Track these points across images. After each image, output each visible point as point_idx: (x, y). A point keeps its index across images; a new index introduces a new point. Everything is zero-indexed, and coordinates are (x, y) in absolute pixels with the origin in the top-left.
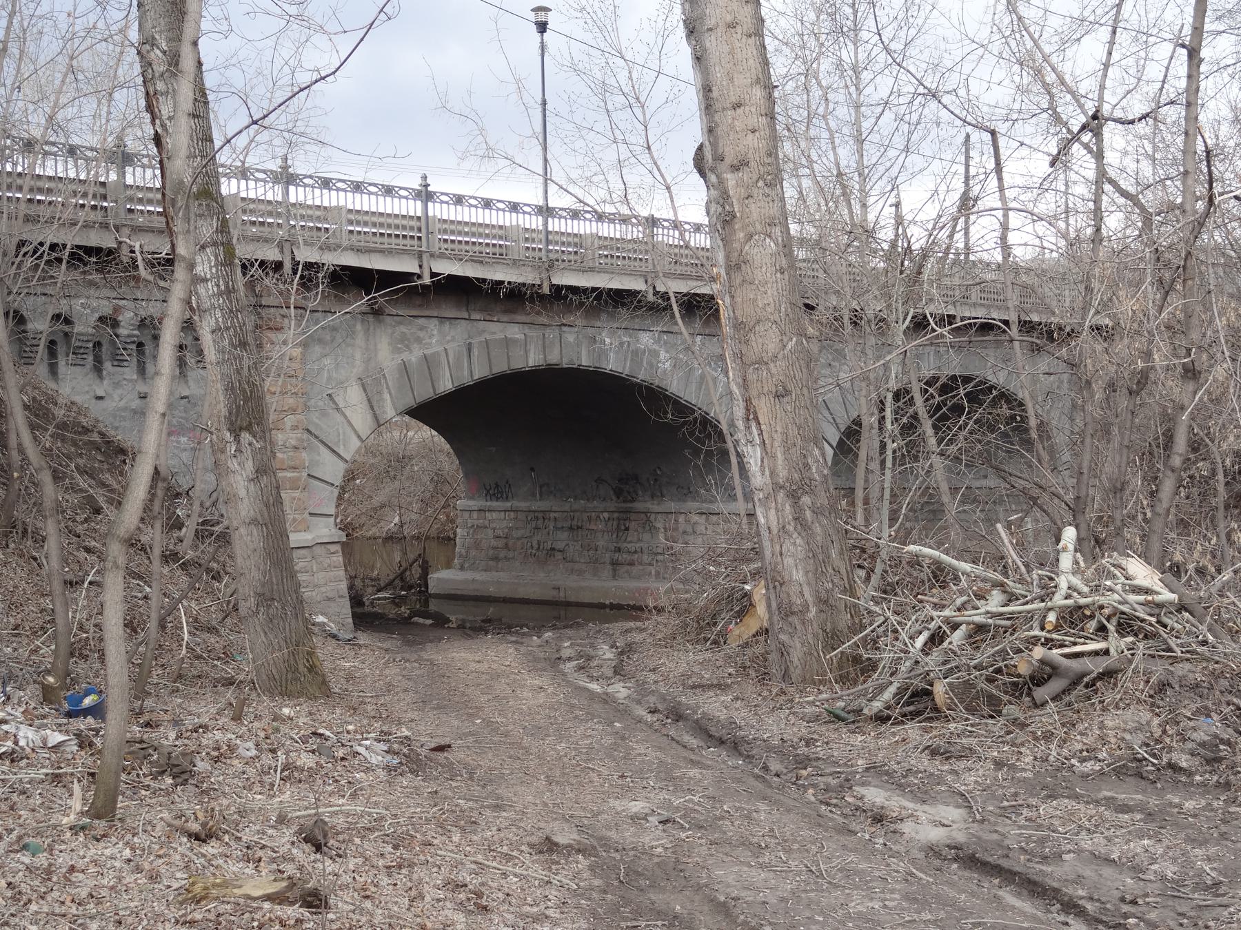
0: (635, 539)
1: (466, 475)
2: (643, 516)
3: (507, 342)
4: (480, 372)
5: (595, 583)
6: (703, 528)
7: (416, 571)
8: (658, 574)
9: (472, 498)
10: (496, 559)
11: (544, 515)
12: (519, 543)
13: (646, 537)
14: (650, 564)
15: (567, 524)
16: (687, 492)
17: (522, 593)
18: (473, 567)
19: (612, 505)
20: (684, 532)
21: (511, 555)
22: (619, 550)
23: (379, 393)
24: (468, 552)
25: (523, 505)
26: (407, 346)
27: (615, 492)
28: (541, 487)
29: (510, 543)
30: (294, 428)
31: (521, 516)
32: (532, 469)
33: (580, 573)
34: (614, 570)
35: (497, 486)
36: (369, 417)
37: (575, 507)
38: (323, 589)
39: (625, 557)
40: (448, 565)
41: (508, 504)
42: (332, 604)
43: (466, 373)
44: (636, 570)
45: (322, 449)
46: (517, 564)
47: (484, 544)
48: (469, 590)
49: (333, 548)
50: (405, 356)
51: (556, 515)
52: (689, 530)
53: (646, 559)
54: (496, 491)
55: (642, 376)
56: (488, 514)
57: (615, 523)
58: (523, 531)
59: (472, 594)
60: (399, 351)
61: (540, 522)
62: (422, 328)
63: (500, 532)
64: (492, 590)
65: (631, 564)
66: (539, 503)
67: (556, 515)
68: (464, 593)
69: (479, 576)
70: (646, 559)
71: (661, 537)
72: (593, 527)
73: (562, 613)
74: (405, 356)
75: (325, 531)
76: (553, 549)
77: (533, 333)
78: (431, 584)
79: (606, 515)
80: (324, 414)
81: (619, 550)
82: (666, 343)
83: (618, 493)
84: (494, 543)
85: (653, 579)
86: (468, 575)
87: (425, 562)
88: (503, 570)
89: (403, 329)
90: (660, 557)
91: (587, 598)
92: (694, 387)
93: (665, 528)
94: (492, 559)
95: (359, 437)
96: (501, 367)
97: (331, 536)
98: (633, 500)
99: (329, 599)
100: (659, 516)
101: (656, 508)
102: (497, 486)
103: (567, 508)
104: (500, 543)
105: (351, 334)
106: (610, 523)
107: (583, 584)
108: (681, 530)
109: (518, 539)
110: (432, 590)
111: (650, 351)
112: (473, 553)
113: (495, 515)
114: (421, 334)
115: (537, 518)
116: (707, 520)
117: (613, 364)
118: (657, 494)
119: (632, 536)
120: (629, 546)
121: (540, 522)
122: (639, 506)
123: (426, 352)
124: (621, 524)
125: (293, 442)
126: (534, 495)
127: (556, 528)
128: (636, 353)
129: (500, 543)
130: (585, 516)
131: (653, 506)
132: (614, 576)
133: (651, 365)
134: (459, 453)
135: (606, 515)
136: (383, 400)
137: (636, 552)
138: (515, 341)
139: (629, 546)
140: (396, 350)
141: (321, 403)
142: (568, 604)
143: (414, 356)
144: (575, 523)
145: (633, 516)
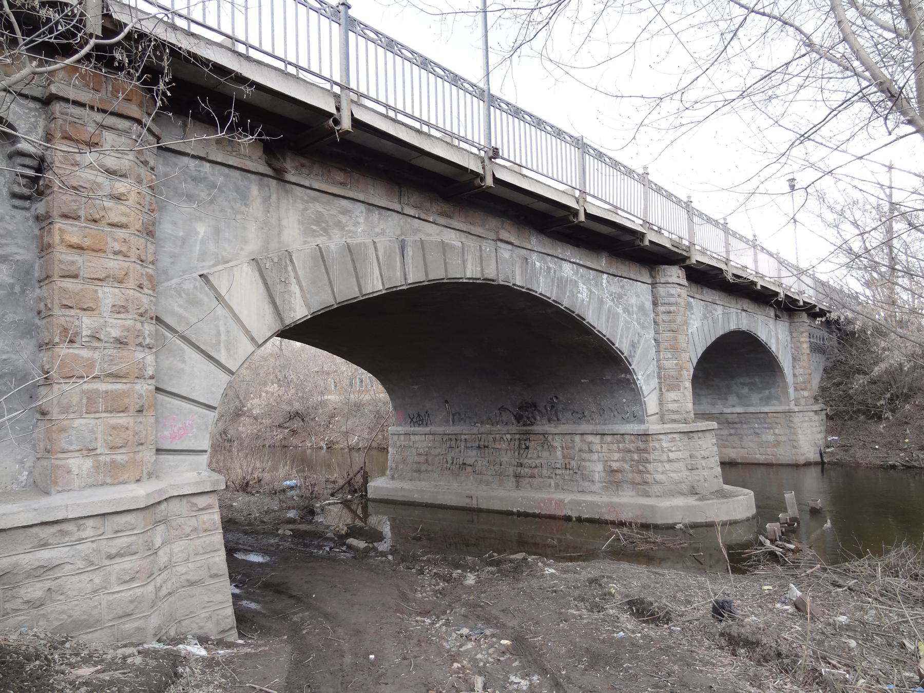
0: (535, 455)
1: (395, 408)
2: (541, 437)
3: (444, 247)
4: (415, 275)
5: (502, 493)
6: (599, 447)
7: (359, 479)
8: (557, 485)
9: (400, 425)
10: (419, 471)
11: (456, 437)
12: (437, 459)
13: (545, 454)
14: (549, 477)
15: (477, 444)
16: (581, 416)
17: (441, 499)
18: (401, 478)
19: (514, 428)
20: (580, 450)
21: (430, 468)
22: (521, 465)
23: (286, 283)
24: (397, 466)
25: (440, 430)
26: (325, 230)
27: (516, 418)
28: (453, 415)
30: (119, 309)
31: (438, 438)
32: (447, 402)
33: (488, 483)
34: (517, 482)
35: (419, 415)
36: (268, 310)
37: (482, 430)
38: (182, 569)
40: (383, 473)
41: (427, 429)
42: (196, 590)
43: (399, 274)
44: (536, 481)
45: (189, 351)
46: (436, 475)
47: (410, 460)
49: (202, 502)
50: (321, 241)
51: (466, 437)
52: (585, 448)
53: (545, 472)
54: (419, 419)
55: (566, 303)
57: (517, 443)
59: (400, 499)
60: (314, 234)
62: (345, 212)
63: (421, 451)
64: (416, 497)
65: (532, 477)
66: (452, 428)
67: (466, 437)
68: (395, 498)
69: (407, 485)
70: (545, 472)
71: (559, 453)
72: (497, 446)
73: (475, 518)
74: (321, 241)
75: (191, 476)
77: (471, 243)
78: (369, 490)
80: (193, 302)
81: (521, 465)
82: (582, 276)
83: (519, 418)
84: (417, 459)
85: (553, 490)
86: (397, 484)
87: (366, 473)
88: (424, 480)
89: (319, 207)
90: (558, 471)
91: (496, 506)
92: (604, 318)
93: (562, 447)
94: (415, 471)
95: (253, 339)
96: (437, 273)
97: (197, 483)
98: (532, 424)
99: (192, 584)
100: (556, 437)
101: (554, 430)
102: (419, 415)
103: (475, 430)
104: (422, 459)
105: (244, 198)
106: (512, 443)
107: (493, 494)
110: (370, 496)
111: (571, 280)
112: (401, 466)
113: (417, 438)
114: (344, 219)
115: (451, 440)
116: (602, 439)
117: (543, 288)
118: (553, 418)
119: (532, 453)
120: (530, 462)
121: (453, 442)
122: (537, 428)
123: (349, 241)
124: (523, 443)
125: (115, 333)
126: (448, 422)
127: (466, 447)
128: (560, 280)
129: (422, 459)
130: (491, 437)
131: (549, 428)
133: (572, 292)
134: (389, 390)
135: (509, 436)
136: (290, 293)
137: (536, 467)
138: (453, 247)
139: (530, 462)
140: (308, 232)
141: (187, 286)
142: (480, 511)
143: (334, 243)
144: (482, 443)
145: (532, 437)
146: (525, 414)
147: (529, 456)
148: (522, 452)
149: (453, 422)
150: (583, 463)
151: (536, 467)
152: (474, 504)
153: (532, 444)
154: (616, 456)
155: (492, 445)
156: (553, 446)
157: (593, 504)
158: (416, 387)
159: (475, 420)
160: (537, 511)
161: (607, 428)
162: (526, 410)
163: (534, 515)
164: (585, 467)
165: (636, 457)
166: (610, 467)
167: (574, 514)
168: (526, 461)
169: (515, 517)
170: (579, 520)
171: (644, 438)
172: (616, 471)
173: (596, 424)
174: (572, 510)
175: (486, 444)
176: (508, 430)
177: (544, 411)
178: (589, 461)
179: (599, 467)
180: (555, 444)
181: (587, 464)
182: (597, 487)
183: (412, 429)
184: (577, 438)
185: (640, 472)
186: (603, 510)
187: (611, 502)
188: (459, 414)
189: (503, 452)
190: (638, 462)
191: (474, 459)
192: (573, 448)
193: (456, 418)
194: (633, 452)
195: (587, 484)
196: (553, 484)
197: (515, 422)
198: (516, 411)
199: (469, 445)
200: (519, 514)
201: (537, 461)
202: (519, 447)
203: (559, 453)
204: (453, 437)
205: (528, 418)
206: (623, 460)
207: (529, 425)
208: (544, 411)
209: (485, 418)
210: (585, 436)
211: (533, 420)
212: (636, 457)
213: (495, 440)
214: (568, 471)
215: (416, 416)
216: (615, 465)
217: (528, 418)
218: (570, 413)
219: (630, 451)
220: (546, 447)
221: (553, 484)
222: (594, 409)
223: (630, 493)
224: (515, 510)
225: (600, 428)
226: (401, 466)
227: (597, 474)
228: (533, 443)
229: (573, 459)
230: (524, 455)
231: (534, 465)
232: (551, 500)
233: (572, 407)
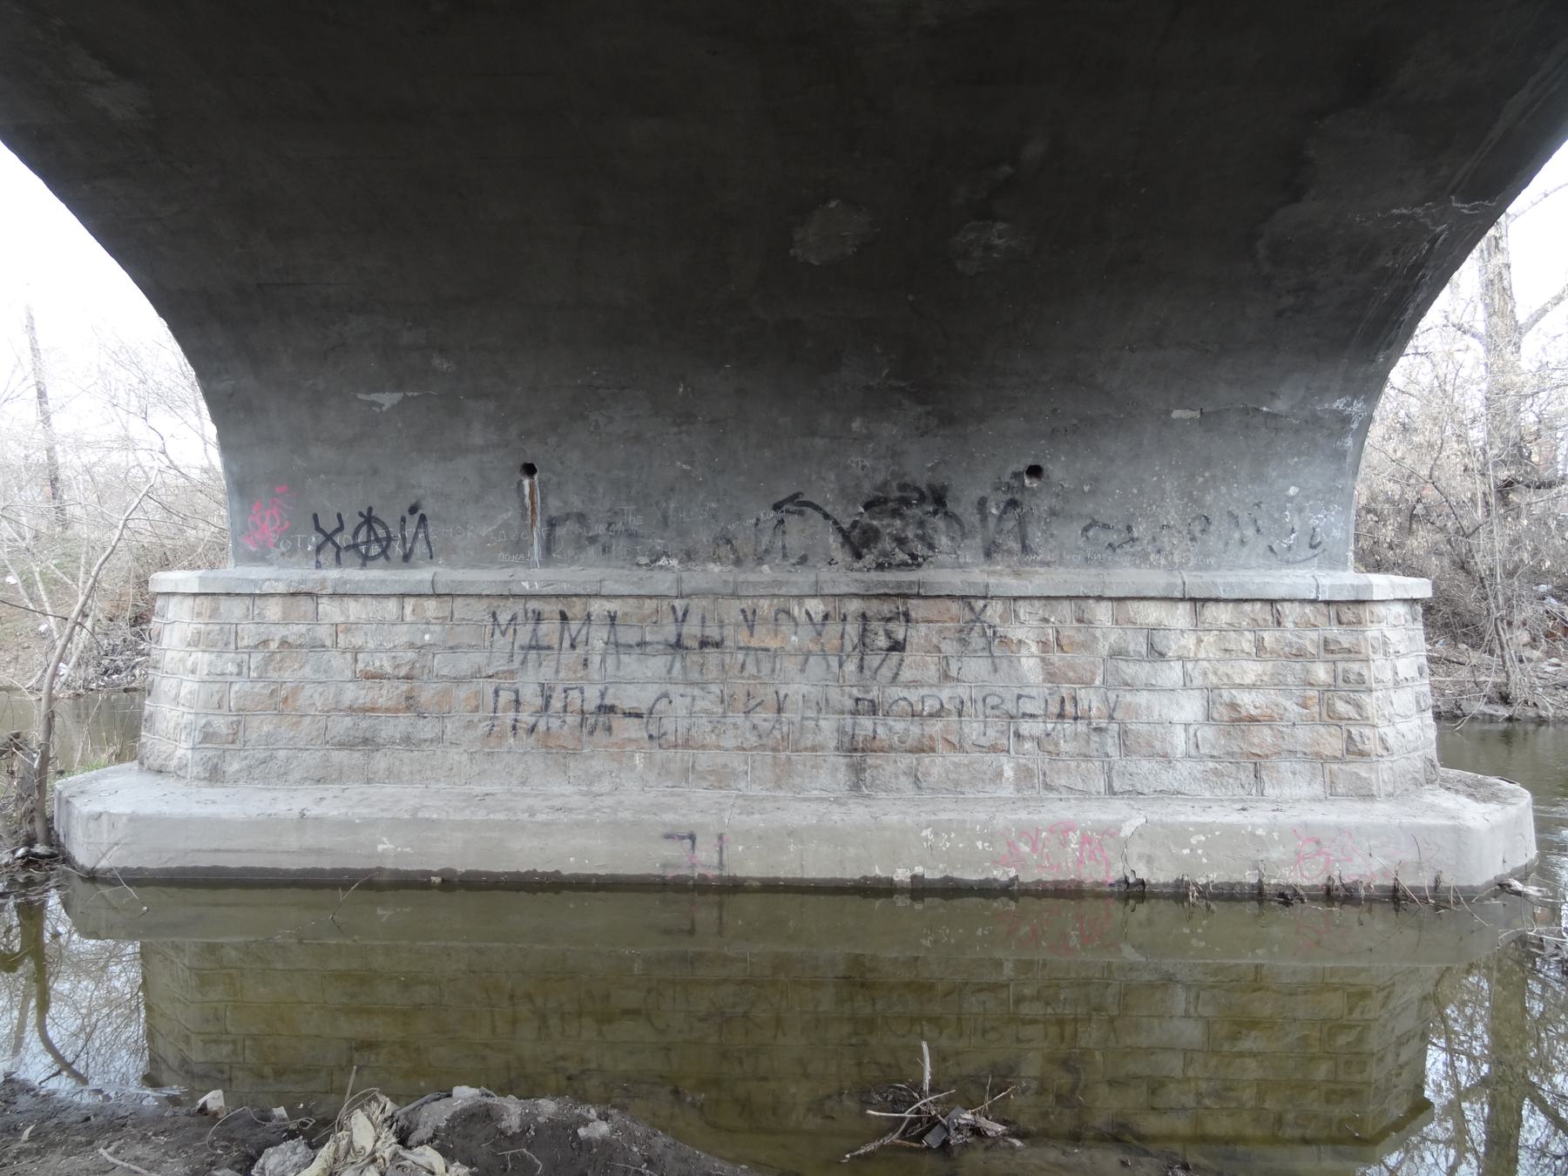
0: (932, 672)
1: (241, 486)
2: (955, 607)
5: (800, 814)
8: (1025, 775)
9: (260, 558)
10: (368, 743)
11: (566, 607)
12: (463, 692)
13: (976, 667)
15: (669, 631)
16: (1121, 539)
18: (264, 771)
19: (844, 577)
20: (1117, 654)
21: (427, 729)
25: (487, 578)
27: (845, 536)
28: (552, 524)
29: (426, 695)
32: (529, 470)
33: (722, 778)
34: (858, 769)
35: (369, 520)
39: (898, 728)
41: (420, 576)
44: (936, 766)
46: (456, 756)
47: (314, 697)
48: (289, 854)
53: (973, 730)
54: (369, 537)
56: (325, 606)
57: (852, 630)
58: (478, 658)
63: (384, 663)
64: (390, 851)
70: (973, 730)
72: (763, 637)
79: (816, 607)
81: (873, 709)
83: (858, 542)
84: (353, 694)
88: (392, 776)
90: (1026, 727)
91: (818, 865)
93: (1044, 645)
98: (915, 562)
100: (1023, 609)
101: (1014, 585)
102: (369, 520)
104: (386, 694)
106: (833, 629)
108: (1103, 648)
109: (458, 680)
112: (261, 726)
115: (538, 617)
119: (916, 664)
120: (914, 695)
121: (549, 629)
122: (941, 575)
124: (883, 626)
129: (386, 694)
130: (732, 610)
132: (856, 787)
135: (816, 607)
137: (938, 714)
139: (914, 695)
142: (734, 887)
144: (692, 629)
145: (917, 608)
146: (889, 524)
147: (906, 674)
148: (873, 660)
149: (548, 548)
150: (1129, 698)
151: (938, 714)
152: (704, 861)
153: (918, 635)
154: (1252, 670)
155: (736, 636)
156: (1004, 641)
157: (1231, 831)
158: (388, 399)
159: (659, 544)
160: (1001, 874)
161: (1223, 580)
162: (896, 513)
163: (987, 890)
164: (1133, 710)
165: (1321, 672)
166: (1233, 706)
167: (1160, 874)
168: (896, 692)
169: (901, 901)
170: (1178, 893)
171: (1348, 614)
172: (1253, 719)
173: (1171, 567)
174: (1150, 860)
175: (713, 632)
176: (811, 584)
177: (971, 517)
178: (1150, 688)
179: (1190, 708)
180: (1016, 633)
181: (1143, 698)
182: (1182, 773)
183: (333, 574)
184: (1102, 614)
185: (1334, 718)
186: (1276, 854)
187: (1306, 825)
188: (581, 518)
189: (791, 665)
190: (1328, 689)
191: (652, 692)
192: (1087, 646)
193: (558, 534)
194: (1313, 659)
195: (1146, 765)
196: (1008, 772)
197: (841, 555)
199: (628, 636)
200: (920, 889)
201: (945, 694)
202: (863, 643)
203: (1030, 665)
204: (551, 608)
205: (901, 541)
206: (1278, 684)
207: (903, 565)
208: (971, 517)
209: (704, 537)
210: (1133, 607)
211: (920, 549)
212: (1321, 672)
213: (750, 620)
214: (1068, 726)
215: (350, 524)
216: (1249, 701)
217: (901, 541)
218: (1077, 527)
219: (1300, 654)
220: (976, 641)
221: (1008, 772)
222: (1172, 517)
223: (1303, 790)
224: (901, 875)
225: (1196, 582)
226: (261, 726)
227: (1180, 730)
228: (923, 628)
229: (1088, 684)
230: (886, 673)
231: (930, 705)
232: (1062, 831)
233: (1090, 507)
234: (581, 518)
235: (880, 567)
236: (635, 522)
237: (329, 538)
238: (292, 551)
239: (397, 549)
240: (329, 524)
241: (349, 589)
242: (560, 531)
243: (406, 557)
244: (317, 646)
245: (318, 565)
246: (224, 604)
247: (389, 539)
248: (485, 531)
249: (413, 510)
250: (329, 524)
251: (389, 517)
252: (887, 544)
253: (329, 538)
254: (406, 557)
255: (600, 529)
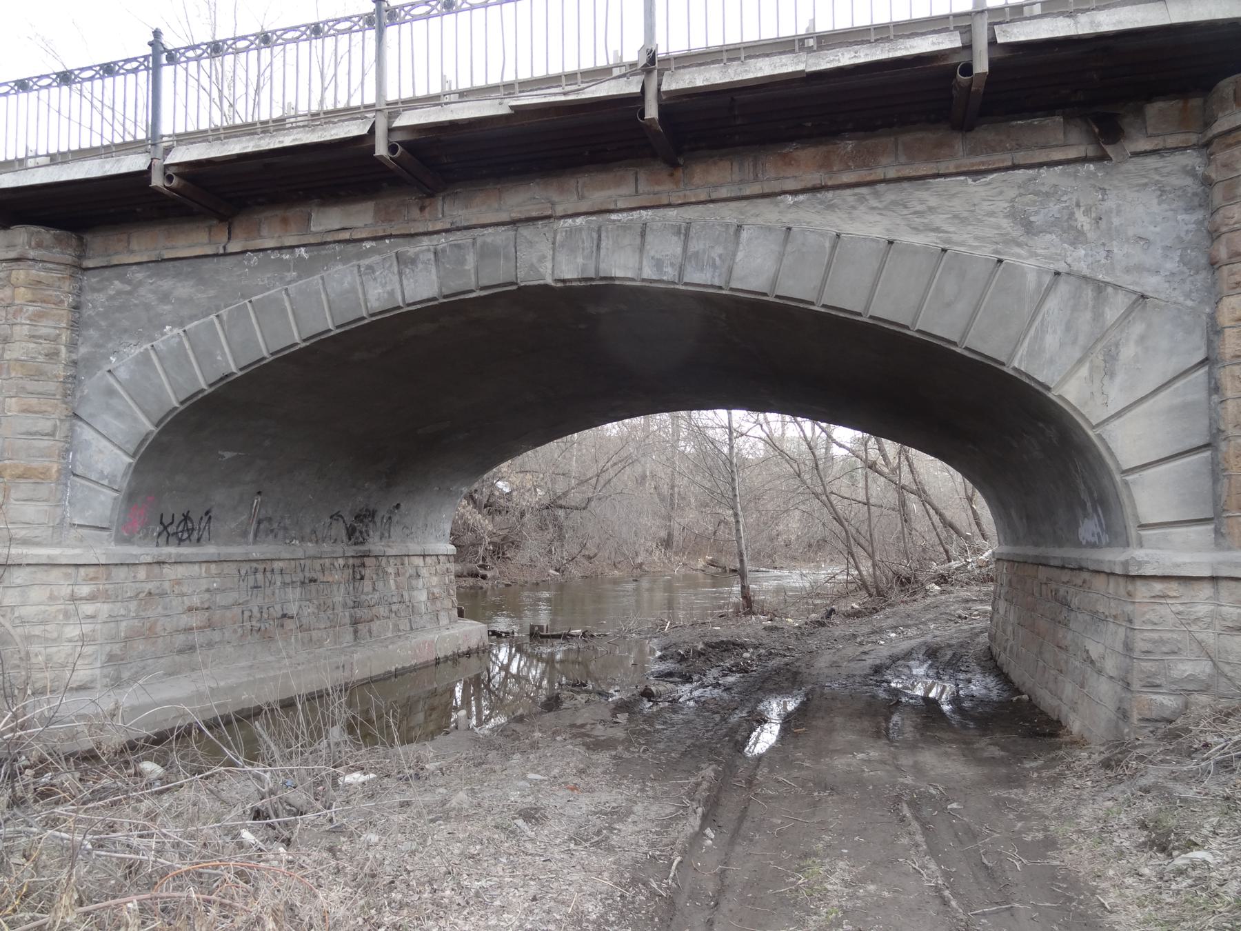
9: (127, 541)
11: (263, 566)
15: (299, 577)
21: (216, 636)
25: (237, 551)
28: (259, 523)
31: (230, 569)
35: (186, 518)
41: (210, 550)
46: (229, 649)
61: (260, 576)
66: (251, 548)
67: (281, 564)
76: (284, 616)
84: (185, 620)
94: (181, 652)
112: (140, 646)
113: (181, 571)
121: (260, 576)
124: (358, 568)
126: (244, 534)
127: (285, 584)
129: (195, 620)
149: (256, 535)
176: (339, 551)
188: (270, 520)
189: (335, 588)
193: (264, 527)
198: (349, 520)
199: (288, 579)
205: (361, 532)
208: (379, 524)
209: (308, 530)
215: (178, 518)
217: (361, 532)
234: (270, 520)
235: (355, 544)
236: (287, 522)
237: (165, 528)
238: (146, 536)
239: (195, 535)
240: (167, 521)
241: (182, 559)
242: (262, 526)
243: (199, 540)
244: (163, 594)
245: (157, 545)
246: (114, 570)
247: (193, 529)
248: (233, 525)
249: (207, 513)
250: (167, 521)
251: (195, 517)
252: (357, 534)
253: (165, 528)
254: (199, 540)
255: (275, 526)
